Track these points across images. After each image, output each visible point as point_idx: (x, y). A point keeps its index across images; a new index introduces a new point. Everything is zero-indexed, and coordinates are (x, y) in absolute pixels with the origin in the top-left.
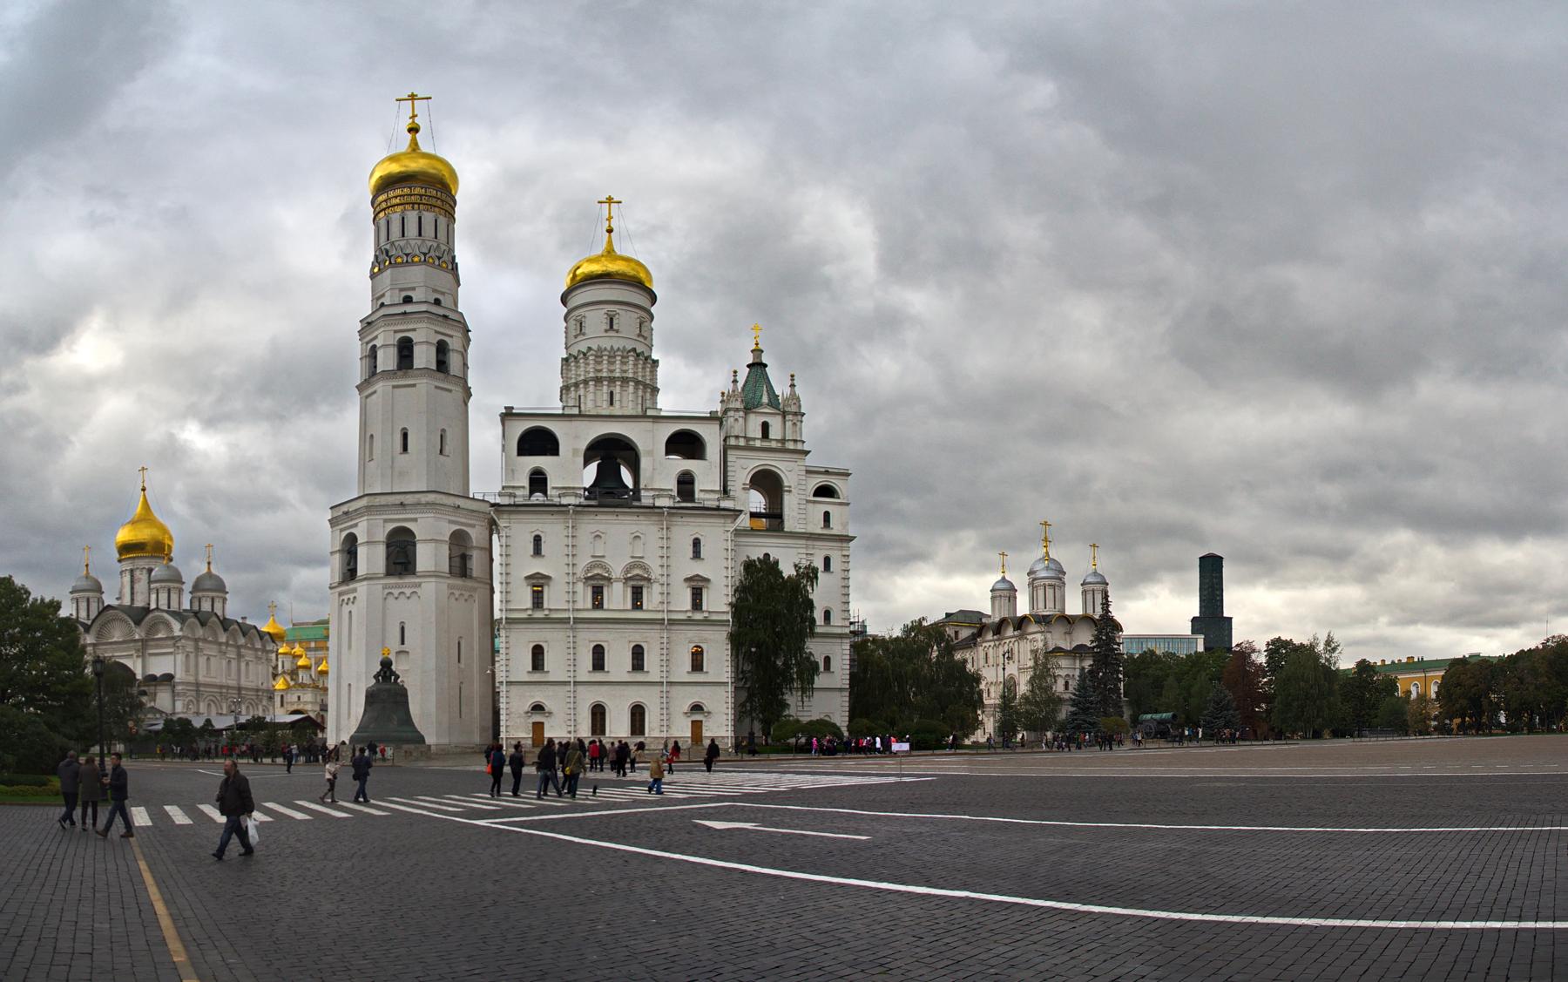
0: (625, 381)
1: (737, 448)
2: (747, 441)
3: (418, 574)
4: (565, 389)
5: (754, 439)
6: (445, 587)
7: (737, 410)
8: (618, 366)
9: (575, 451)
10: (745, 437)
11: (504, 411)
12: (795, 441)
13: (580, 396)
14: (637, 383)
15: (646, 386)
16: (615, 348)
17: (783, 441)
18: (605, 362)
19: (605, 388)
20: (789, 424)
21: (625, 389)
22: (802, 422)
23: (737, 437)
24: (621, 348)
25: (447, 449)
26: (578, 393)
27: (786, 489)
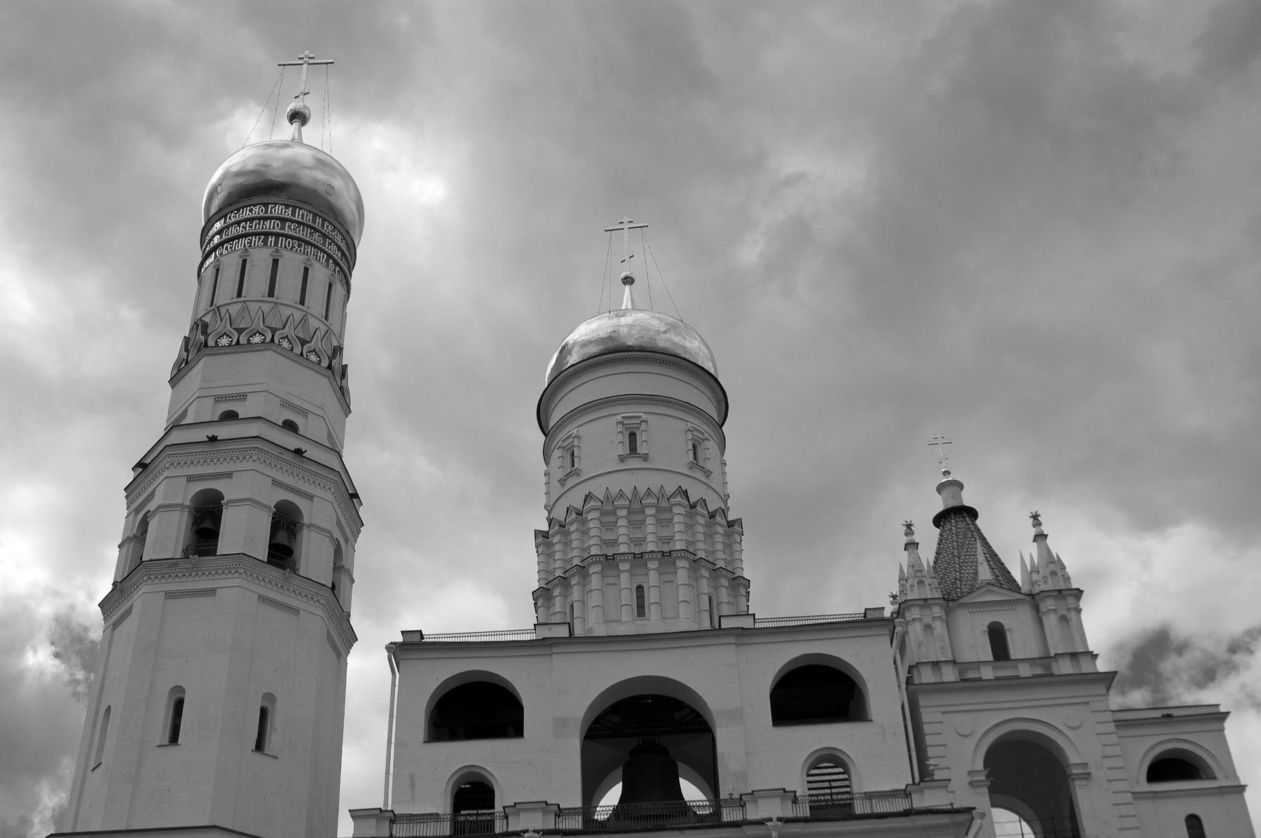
0: (667, 557)
1: (940, 688)
2: (960, 673)
4: (542, 596)
5: (978, 664)
7: (925, 603)
8: (650, 529)
9: (561, 724)
10: (954, 662)
11: (400, 639)
12: (1074, 656)
13: (572, 606)
14: (696, 562)
15: (715, 571)
16: (642, 491)
17: (1046, 659)
18: (622, 522)
19: (625, 578)
20: (1051, 621)
21: (668, 577)
22: (1079, 611)
23: (936, 664)
24: (655, 490)
25: (274, 740)
26: (569, 600)
27: (1074, 772)
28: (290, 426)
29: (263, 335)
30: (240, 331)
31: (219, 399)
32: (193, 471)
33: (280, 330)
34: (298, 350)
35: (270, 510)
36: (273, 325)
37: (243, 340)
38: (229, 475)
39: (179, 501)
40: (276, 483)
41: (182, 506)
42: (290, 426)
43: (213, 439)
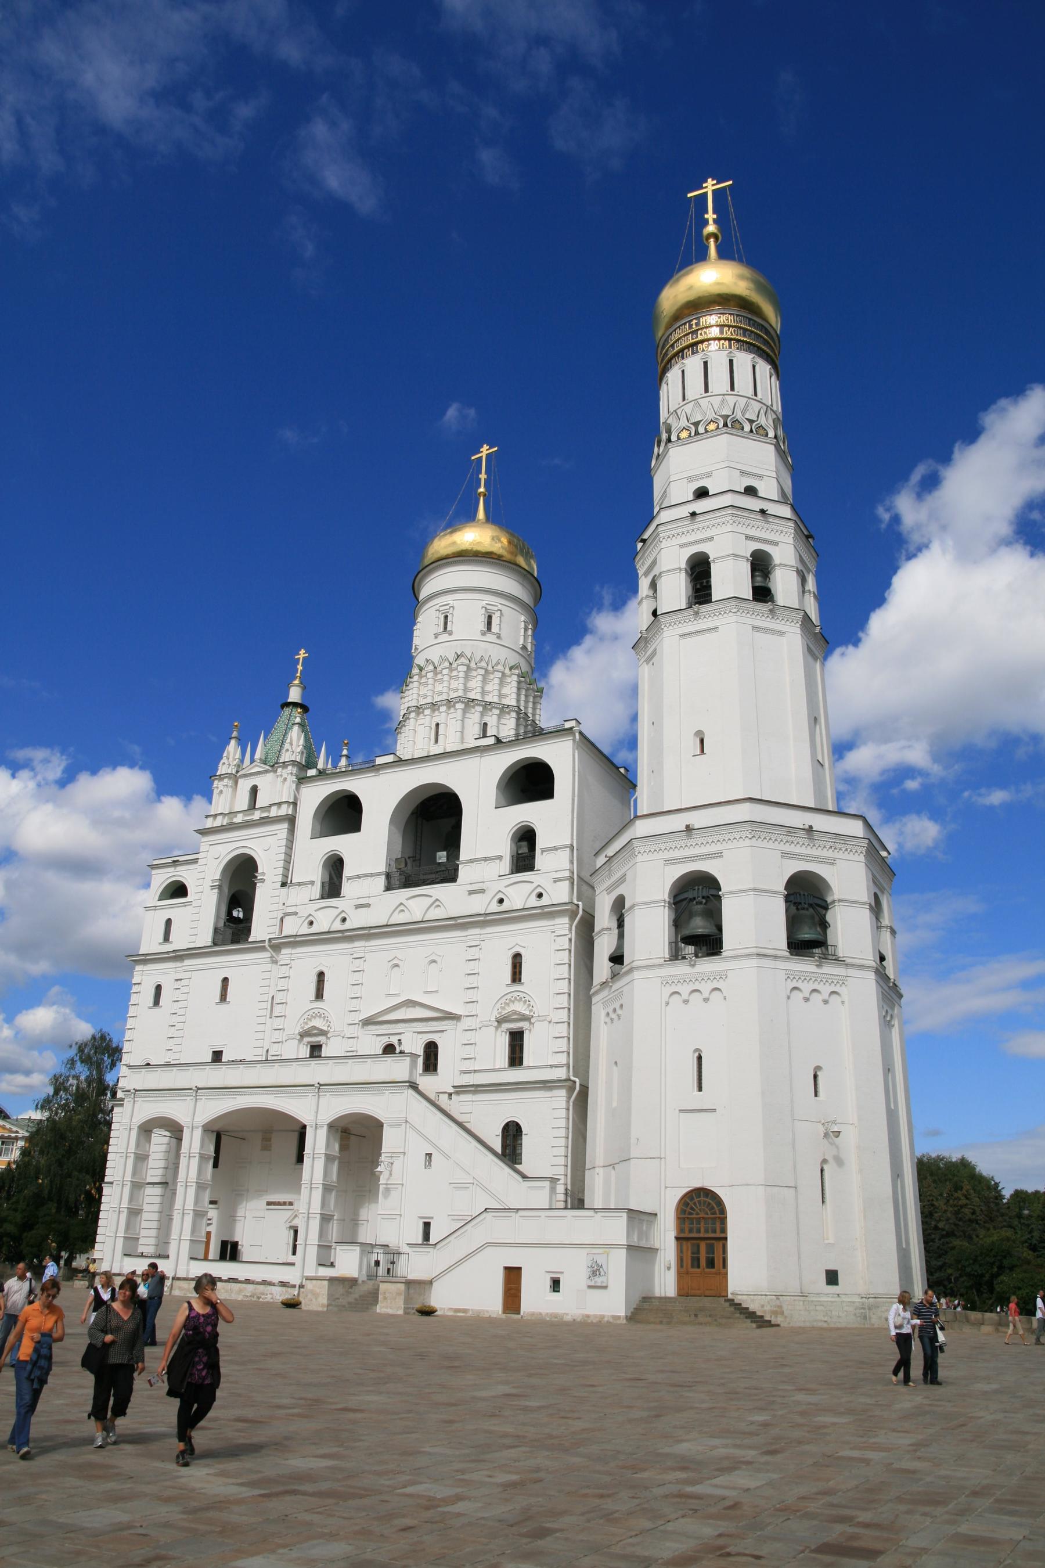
3: (724, 954)
6: (782, 975)
28: (751, 491)
29: (716, 422)
30: (696, 424)
31: (690, 479)
32: (684, 539)
33: (729, 416)
34: (747, 428)
35: (748, 560)
36: (724, 413)
37: (701, 430)
38: (711, 539)
39: (677, 566)
40: (748, 537)
41: (680, 569)
42: (751, 491)
43: (693, 514)
